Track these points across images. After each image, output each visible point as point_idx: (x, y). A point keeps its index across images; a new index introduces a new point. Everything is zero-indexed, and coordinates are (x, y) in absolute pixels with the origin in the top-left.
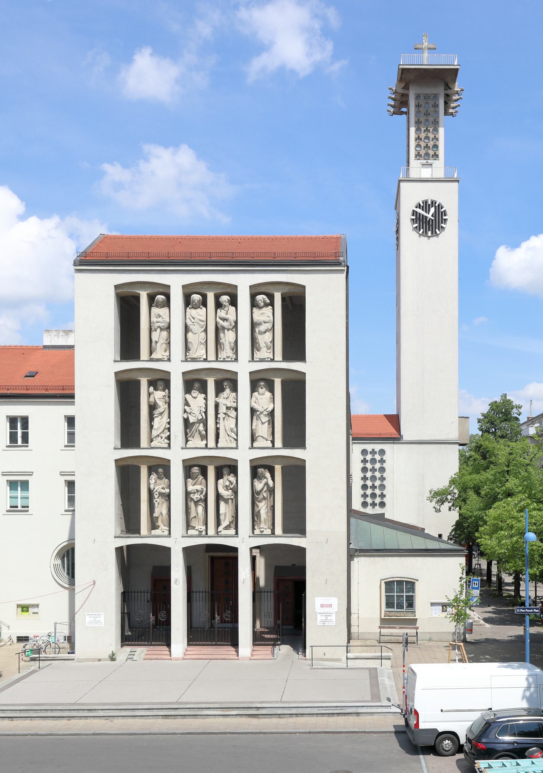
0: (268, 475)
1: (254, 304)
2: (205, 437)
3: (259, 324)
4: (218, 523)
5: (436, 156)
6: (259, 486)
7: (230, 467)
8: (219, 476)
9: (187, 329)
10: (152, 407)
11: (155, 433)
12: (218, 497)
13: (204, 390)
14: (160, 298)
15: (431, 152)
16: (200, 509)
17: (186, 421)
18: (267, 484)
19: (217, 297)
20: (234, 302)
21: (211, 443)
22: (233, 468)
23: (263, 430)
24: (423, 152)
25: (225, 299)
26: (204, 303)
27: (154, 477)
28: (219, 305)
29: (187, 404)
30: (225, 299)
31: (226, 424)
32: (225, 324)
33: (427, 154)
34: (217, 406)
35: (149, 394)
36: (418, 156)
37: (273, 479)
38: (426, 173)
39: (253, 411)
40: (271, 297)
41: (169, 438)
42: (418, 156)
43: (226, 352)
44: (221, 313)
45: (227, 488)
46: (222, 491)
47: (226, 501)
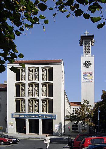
0: (45, 102)
1: (43, 71)
2: (32, 95)
3: (44, 74)
4: (35, 111)
5: (89, 53)
6: (43, 104)
7: (37, 100)
8: (35, 102)
9: (29, 75)
10: (22, 90)
11: (22, 94)
12: (35, 106)
13: (32, 86)
14: (24, 70)
15: (88, 52)
16: (32, 108)
17: (29, 92)
18: (45, 104)
19: (35, 70)
20: (38, 71)
21: (34, 96)
22: (37, 101)
23: (45, 94)
24: (86, 52)
25: (37, 70)
26: (32, 71)
27: (22, 102)
28: (35, 71)
29: (29, 89)
30: (37, 70)
31: (37, 93)
32: (37, 74)
33: (87, 52)
34: (35, 89)
35: (21, 87)
36: (85, 53)
37: (46, 103)
38: (87, 56)
39: (42, 90)
40: (46, 69)
41: (25, 95)
42: (85, 53)
43: (37, 79)
44: (36, 72)
45: (36, 104)
46: (36, 105)
47: (37, 107)
